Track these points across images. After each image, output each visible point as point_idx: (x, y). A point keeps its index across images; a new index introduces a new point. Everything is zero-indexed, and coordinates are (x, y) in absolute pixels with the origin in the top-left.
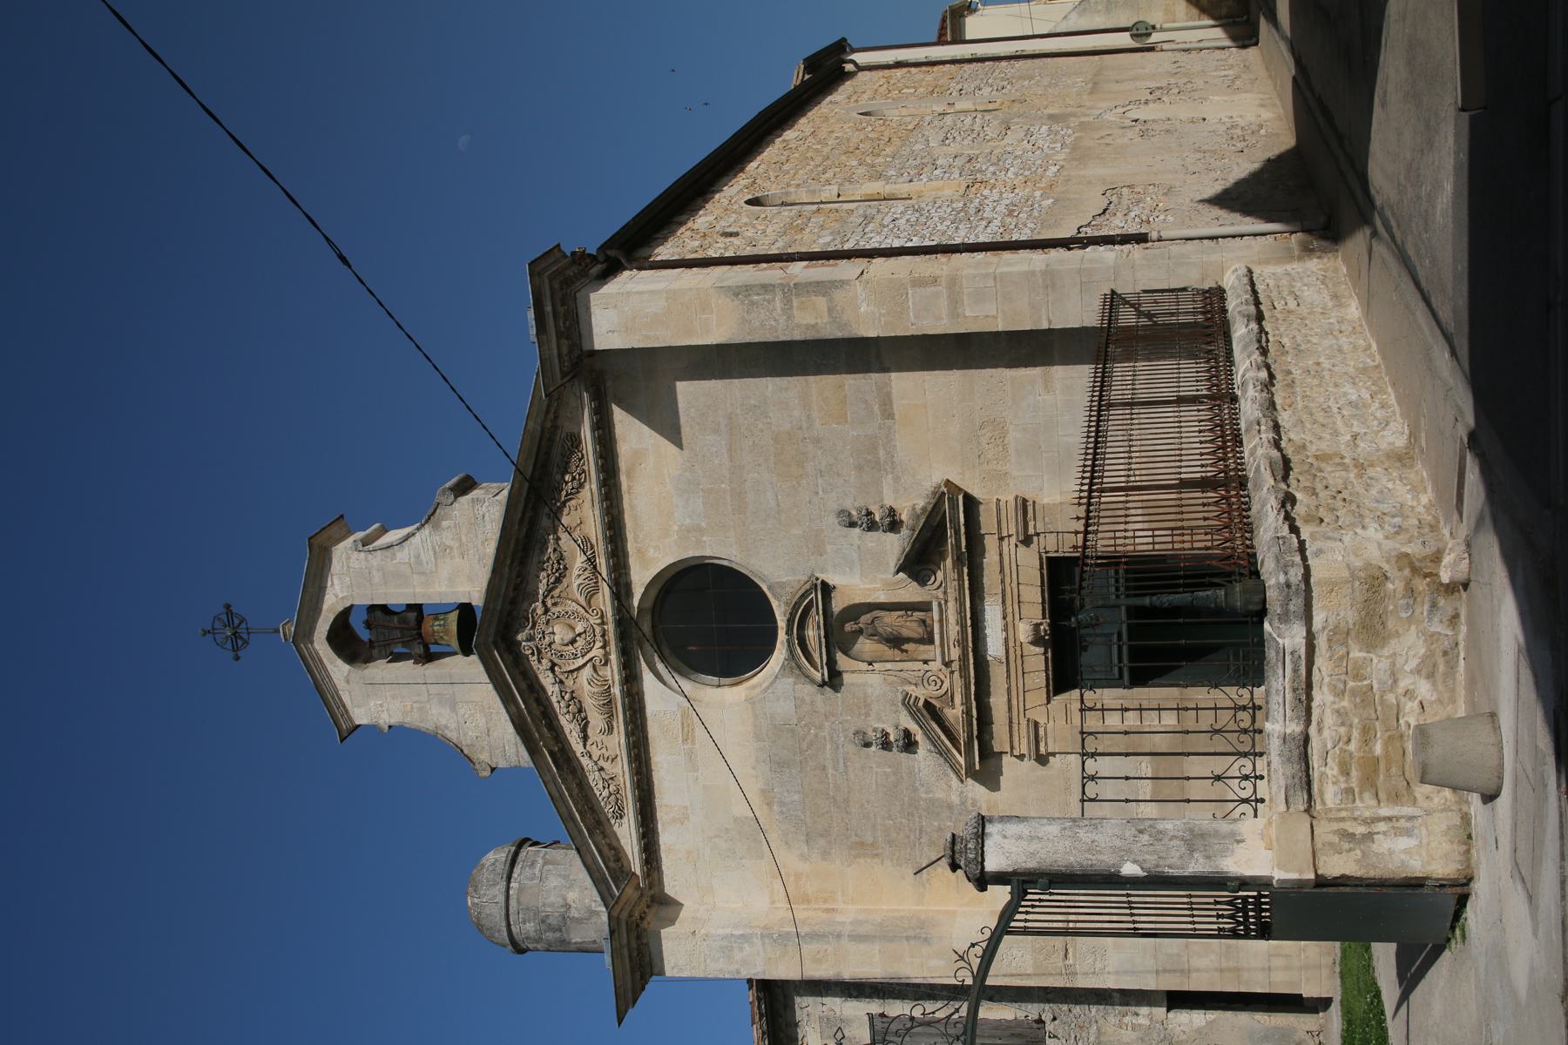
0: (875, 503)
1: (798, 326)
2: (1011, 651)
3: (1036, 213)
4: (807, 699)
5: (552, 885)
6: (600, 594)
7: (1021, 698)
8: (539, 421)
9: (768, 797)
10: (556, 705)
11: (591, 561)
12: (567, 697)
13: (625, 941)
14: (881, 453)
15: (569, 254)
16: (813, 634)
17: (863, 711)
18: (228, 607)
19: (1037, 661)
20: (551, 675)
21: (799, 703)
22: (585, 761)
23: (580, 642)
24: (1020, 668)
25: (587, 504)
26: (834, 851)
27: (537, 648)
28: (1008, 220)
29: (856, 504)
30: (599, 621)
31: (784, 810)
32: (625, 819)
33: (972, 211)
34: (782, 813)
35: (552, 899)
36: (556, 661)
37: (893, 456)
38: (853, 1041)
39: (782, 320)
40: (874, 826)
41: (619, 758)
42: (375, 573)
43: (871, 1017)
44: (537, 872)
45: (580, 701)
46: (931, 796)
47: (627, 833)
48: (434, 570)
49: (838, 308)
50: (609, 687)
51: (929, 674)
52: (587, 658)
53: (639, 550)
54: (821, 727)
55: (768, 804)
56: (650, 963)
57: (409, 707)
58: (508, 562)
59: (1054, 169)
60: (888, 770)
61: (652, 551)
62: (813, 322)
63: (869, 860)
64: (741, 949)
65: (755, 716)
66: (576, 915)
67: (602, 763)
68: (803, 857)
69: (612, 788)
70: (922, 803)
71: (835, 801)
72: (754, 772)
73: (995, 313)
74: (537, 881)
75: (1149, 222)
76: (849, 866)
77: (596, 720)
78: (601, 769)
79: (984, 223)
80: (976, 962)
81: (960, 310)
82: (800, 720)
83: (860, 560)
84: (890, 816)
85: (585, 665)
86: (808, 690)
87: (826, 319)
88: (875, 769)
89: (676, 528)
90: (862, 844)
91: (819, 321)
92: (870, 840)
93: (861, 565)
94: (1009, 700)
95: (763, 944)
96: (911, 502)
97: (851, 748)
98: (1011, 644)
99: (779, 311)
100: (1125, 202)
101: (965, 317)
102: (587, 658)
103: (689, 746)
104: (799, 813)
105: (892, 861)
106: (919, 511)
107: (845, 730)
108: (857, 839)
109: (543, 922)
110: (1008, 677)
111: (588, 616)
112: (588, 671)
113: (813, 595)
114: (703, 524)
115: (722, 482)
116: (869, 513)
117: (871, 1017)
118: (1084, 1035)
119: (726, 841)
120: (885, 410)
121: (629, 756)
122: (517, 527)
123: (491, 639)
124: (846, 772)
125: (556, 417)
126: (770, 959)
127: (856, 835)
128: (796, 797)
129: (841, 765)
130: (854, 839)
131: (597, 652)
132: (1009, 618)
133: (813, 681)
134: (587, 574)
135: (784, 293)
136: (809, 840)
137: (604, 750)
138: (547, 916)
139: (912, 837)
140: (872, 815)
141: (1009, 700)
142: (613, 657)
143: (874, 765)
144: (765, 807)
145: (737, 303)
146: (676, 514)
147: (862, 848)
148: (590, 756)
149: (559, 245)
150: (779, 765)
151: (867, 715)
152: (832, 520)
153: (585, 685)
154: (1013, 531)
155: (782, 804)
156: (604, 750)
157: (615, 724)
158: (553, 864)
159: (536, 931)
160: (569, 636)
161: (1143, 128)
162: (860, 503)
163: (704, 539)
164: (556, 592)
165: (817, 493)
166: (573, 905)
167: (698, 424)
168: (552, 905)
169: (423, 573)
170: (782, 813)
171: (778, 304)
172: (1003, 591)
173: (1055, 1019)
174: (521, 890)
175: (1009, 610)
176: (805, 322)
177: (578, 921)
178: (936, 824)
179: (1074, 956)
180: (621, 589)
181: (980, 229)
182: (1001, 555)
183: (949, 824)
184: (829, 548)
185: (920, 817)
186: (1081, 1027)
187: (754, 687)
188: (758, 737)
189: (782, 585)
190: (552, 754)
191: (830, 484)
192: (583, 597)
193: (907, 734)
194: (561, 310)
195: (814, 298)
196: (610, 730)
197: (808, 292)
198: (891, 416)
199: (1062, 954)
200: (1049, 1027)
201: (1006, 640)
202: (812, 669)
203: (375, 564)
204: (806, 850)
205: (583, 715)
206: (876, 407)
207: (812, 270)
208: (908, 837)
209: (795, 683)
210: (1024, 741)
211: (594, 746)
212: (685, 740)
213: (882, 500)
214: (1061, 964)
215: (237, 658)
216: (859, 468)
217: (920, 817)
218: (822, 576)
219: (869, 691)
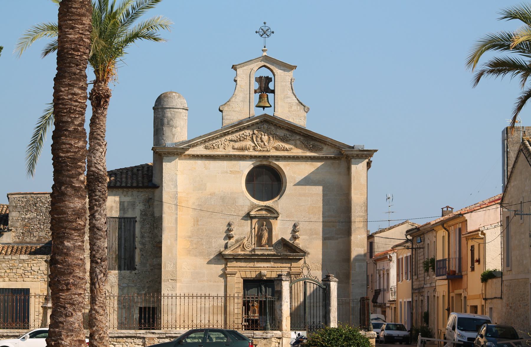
2: (258, 268)
4: (243, 209)
6: (275, 151)
7: (243, 270)
8: (329, 141)
9: (212, 194)
13: (178, 151)
14: (315, 236)
16: (264, 213)
17: (239, 225)
18: (273, 32)
19: (253, 275)
22: (223, 139)
23: (262, 144)
24: (252, 270)
26: (196, 212)
29: (300, 228)
31: (209, 199)
38: (127, 212)
39: (357, 215)
40: (204, 225)
41: (225, 150)
42: (285, 83)
44: (184, 118)
46: (213, 243)
47: (200, 150)
48: (285, 102)
55: (211, 194)
56: (168, 156)
57: (243, 87)
58: (289, 127)
60: (221, 231)
64: (172, 185)
68: (194, 203)
69: (216, 147)
70: (211, 240)
76: (191, 217)
77: (237, 145)
80: (316, 280)
82: (237, 206)
87: (357, 226)
88: (221, 227)
89: (295, 176)
90: (198, 221)
92: (199, 223)
94: (243, 267)
95: (174, 192)
96: (300, 243)
98: (259, 268)
99: (360, 214)
101: (355, 263)
102: (257, 145)
103: (229, 172)
105: (193, 229)
106: (299, 245)
107: (234, 219)
109: (171, 119)
110: (250, 267)
115: (308, 191)
118: (131, 282)
122: (299, 130)
123: (266, 118)
124: (221, 218)
125: (329, 145)
126: (169, 193)
127: (201, 220)
128: (213, 203)
130: (199, 219)
132: (267, 268)
138: (173, 121)
139: (200, 236)
141: (243, 267)
144: (210, 193)
145: (362, 203)
147: (196, 221)
150: (223, 199)
151: (238, 226)
154: (292, 271)
156: (227, 146)
159: (168, 116)
165: (304, 217)
166: (176, 129)
169: (284, 99)
170: (208, 198)
171: (361, 214)
172: (275, 267)
173: (135, 274)
174: (180, 113)
175: (269, 268)
177: (171, 131)
178: (204, 243)
179: (172, 282)
180: (278, 158)
183: (204, 247)
185: (206, 239)
186: (133, 281)
187: (246, 193)
189: (278, 205)
190: (229, 131)
194: (364, 156)
199: (172, 279)
200: (134, 272)
201: (261, 267)
203: (287, 84)
208: (200, 235)
209: (248, 206)
210: (231, 271)
212: (231, 171)
214: (169, 278)
215: (256, 32)
216: (311, 230)
217: (206, 239)
218: (280, 216)
219: (245, 227)
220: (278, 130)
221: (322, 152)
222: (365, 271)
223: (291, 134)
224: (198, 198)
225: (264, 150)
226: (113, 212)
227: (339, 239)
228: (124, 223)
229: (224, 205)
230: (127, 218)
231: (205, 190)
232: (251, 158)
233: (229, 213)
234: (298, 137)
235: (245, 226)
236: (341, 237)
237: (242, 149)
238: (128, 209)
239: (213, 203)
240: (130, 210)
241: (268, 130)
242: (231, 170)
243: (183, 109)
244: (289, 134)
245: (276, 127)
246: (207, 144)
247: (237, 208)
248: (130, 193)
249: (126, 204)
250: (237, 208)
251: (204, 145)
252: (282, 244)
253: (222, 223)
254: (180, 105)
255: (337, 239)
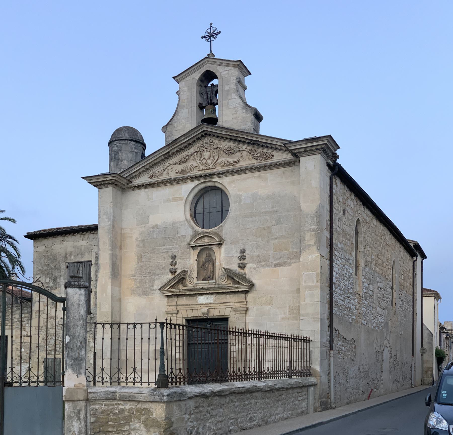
0: (247, 261)
1: (305, 234)
3: (346, 316)
5: (129, 155)
6: (220, 168)
9: (156, 226)
10: (184, 154)
11: (230, 164)
12: (187, 158)
15: (336, 152)
16: (205, 241)
20: (194, 151)
21: (184, 237)
22: (167, 164)
23: (204, 161)
25: (250, 162)
27: (203, 146)
28: (343, 307)
30: (211, 168)
32: (149, 179)
33: (348, 295)
34: (150, 232)
35: (124, 155)
36: (199, 153)
37: (262, 267)
43: (91, 261)
44: (134, 150)
45: (185, 162)
47: (144, 179)
49: (310, 248)
50: (190, 172)
51: (193, 279)
52: (200, 164)
53: (234, 181)
54: (176, 244)
55: (153, 227)
59: (365, 323)
60: (164, 266)
61: (234, 185)
62: (306, 239)
63: (137, 260)
64: (107, 218)
65: (181, 222)
66: (119, 164)
67: (166, 170)
68: (137, 239)
71: (154, 249)
72: (163, 222)
73: (306, 301)
74: (130, 150)
75: (339, 353)
77: (179, 168)
78: (164, 170)
79: (343, 299)
81: (308, 289)
82: (179, 237)
83: (229, 256)
84: (150, 266)
85: (197, 163)
86: (188, 239)
89: (241, 194)
90: (142, 258)
91: (306, 241)
92: (143, 260)
93: (227, 257)
95: (108, 225)
96: (248, 272)
97: (170, 254)
100: (348, 346)
104: (150, 237)
108: (143, 256)
111: (213, 164)
112: (195, 164)
113: (218, 241)
114: (242, 203)
116: (244, 259)
117: (91, 261)
119: (142, 213)
120: (277, 265)
121: (168, 179)
124: (163, 252)
126: (104, 228)
128: (155, 236)
129: (165, 251)
130: (143, 255)
131: (201, 167)
133: (191, 241)
134: (226, 162)
135: (316, 229)
136: (143, 240)
137: (170, 171)
138: (119, 154)
140: (150, 261)
142: (200, 172)
143: (165, 261)
144: (152, 226)
146: (245, 193)
147: (140, 257)
148: (168, 166)
149: (339, 148)
151: (181, 259)
152: (242, 247)
153: (192, 163)
155: (153, 231)
157: (178, 174)
158: (136, 155)
160: (206, 158)
161: (380, 352)
162: (247, 256)
163: (237, 204)
164: (222, 152)
166: (122, 162)
167: (275, 201)
168: (122, 155)
176: (306, 236)
177: (117, 165)
181: (340, 298)
182: (229, 303)
184: (233, 246)
188: (174, 223)
189: (222, 230)
190: (168, 152)
191: (254, 246)
192: (219, 162)
193: (175, 272)
195: (314, 239)
196: (177, 173)
197: (316, 237)
198: (275, 266)
202: (194, 241)
204: (139, 240)
205: (181, 163)
206: (278, 261)
207: (325, 239)
209: (190, 235)
211: (171, 168)
212: (173, 198)
213: (248, 263)
216: (258, 256)
219: (188, 260)
220: (222, 143)
221: (273, 159)
222: (317, 301)
223: (236, 145)
224: (141, 233)
225: (206, 169)
226: (73, 257)
227: (292, 265)
228: (82, 267)
229: (166, 238)
230: (84, 262)
231: (148, 223)
232: (193, 181)
233: (171, 245)
234: (244, 147)
235: (187, 258)
236: (295, 262)
237: (183, 172)
238: (85, 252)
239: (155, 236)
240: (86, 254)
241: (211, 145)
242: (173, 197)
243: (131, 140)
244: (234, 145)
245: (219, 139)
246: (151, 172)
247: (179, 239)
248: (86, 236)
249: (83, 249)
250: (179, 239)
251: (148, 175)
252: (226, 275)
253: (164, 258)
254: (127, 135)
255: (290, 264)
